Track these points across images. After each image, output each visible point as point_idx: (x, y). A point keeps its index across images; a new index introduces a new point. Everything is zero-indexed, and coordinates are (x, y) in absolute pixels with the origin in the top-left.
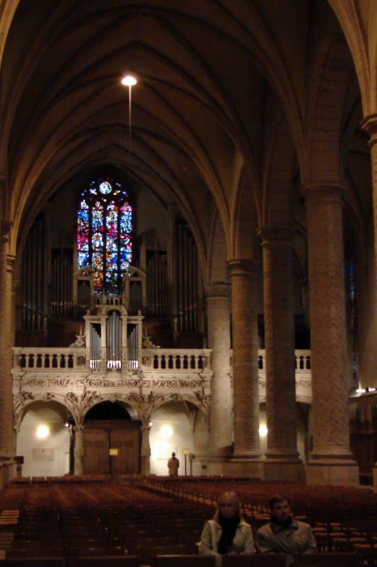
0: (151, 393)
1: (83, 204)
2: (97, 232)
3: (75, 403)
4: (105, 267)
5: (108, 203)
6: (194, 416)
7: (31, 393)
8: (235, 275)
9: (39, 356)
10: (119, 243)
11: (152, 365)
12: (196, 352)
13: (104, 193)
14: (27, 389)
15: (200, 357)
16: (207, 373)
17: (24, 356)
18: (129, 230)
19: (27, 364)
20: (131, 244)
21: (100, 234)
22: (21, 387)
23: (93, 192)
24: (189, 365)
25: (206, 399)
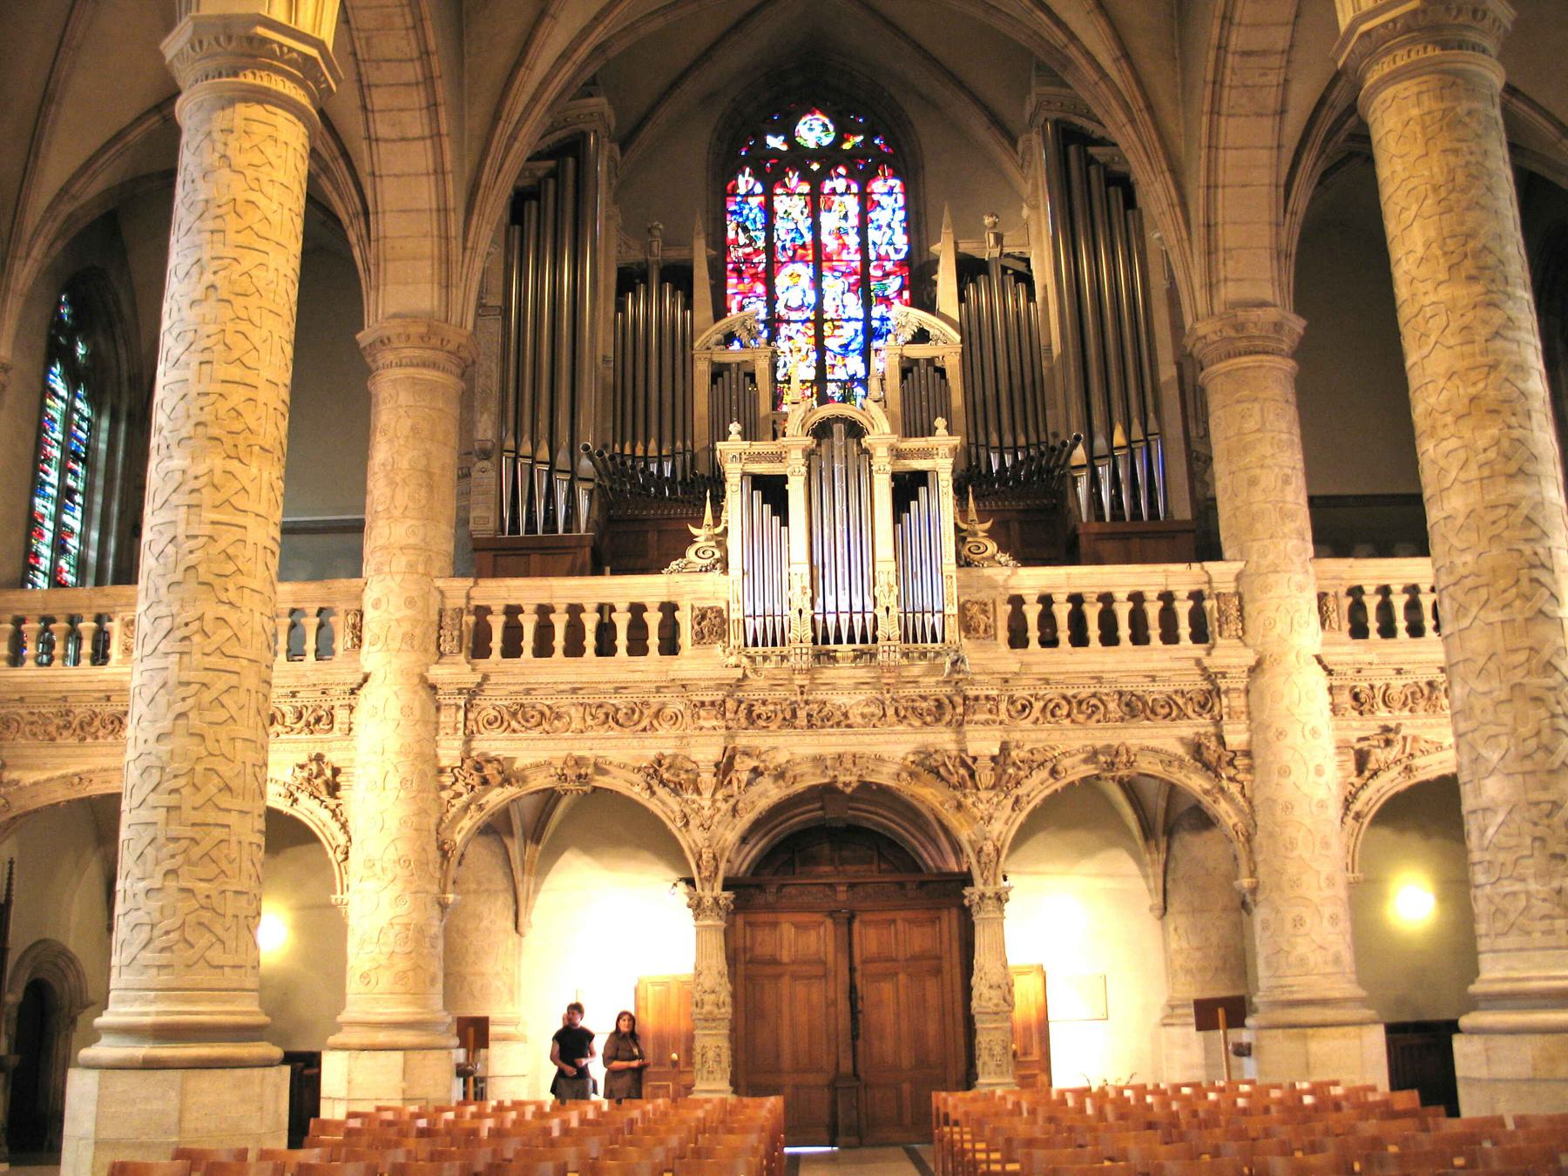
0: (1005, 747)
1: (745, 181)
2: (792, 260)
3: (691, 796)
4: (821, 367)
5: (825, 174)
6: (1162, 857)
7: (512, 760)
8: (1394, 77)
9: (544, 611)
10: (863, 285)
11: (1003, 634)
12: (1181, 578)
13: (812, 145)
14: (492, 744)
15: (1197, 597)
16: (1229, 655)
17: (482, 612)
18: (897, 251)
19: (496, 643)
20: (906, 295)
21: (799, 267)
22: (469, 738)
23: (775, 142)
24: (1155, 632)
25: (1231, 763)
